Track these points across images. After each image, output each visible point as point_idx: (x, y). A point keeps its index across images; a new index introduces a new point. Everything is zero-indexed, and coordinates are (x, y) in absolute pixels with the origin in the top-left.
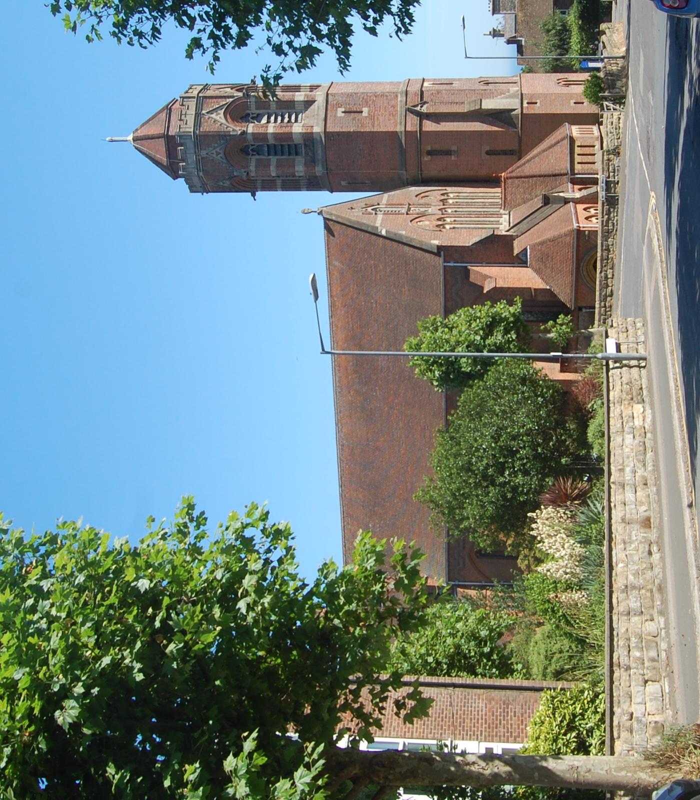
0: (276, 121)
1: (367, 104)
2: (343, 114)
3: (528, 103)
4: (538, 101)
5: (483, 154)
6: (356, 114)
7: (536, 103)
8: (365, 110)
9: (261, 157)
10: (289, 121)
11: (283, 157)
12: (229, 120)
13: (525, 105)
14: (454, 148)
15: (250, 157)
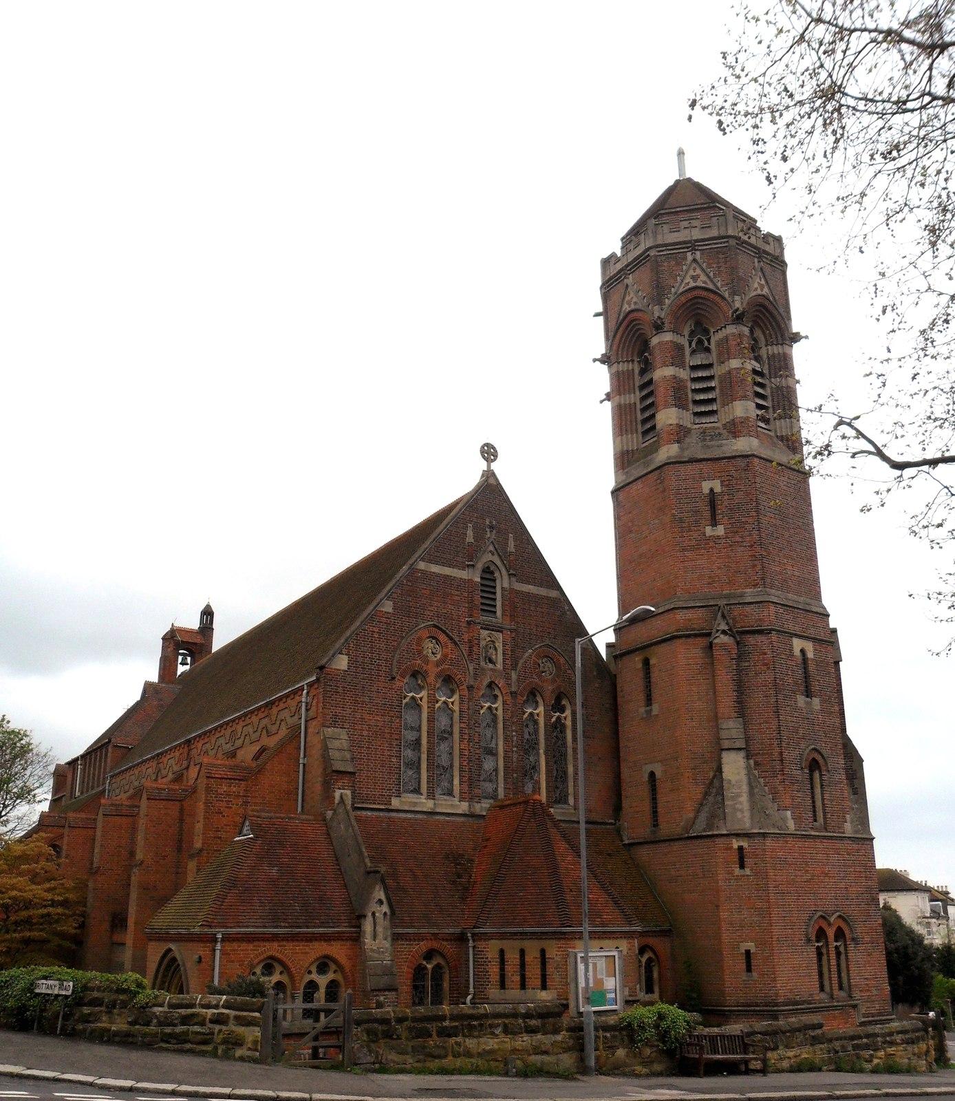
0: (694, 380)
1: (733, 531)
2: (706, 491)
3: (741, 849)
4: (748, 871)
5: (649, 768)
6: (707, 514)
7: (742, 866)
8: (720, 530)
9: (637, 376)
10: (696, 402)
11: (639, 413)
12: (683, 299)
13: (735, 844)
14: (655, 709)
15: (636, 359)
